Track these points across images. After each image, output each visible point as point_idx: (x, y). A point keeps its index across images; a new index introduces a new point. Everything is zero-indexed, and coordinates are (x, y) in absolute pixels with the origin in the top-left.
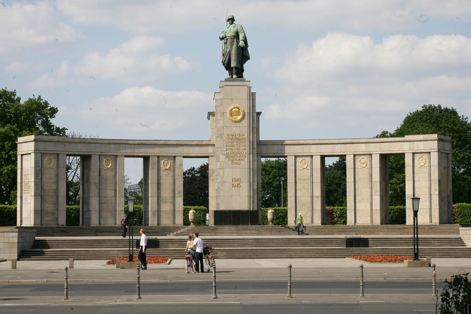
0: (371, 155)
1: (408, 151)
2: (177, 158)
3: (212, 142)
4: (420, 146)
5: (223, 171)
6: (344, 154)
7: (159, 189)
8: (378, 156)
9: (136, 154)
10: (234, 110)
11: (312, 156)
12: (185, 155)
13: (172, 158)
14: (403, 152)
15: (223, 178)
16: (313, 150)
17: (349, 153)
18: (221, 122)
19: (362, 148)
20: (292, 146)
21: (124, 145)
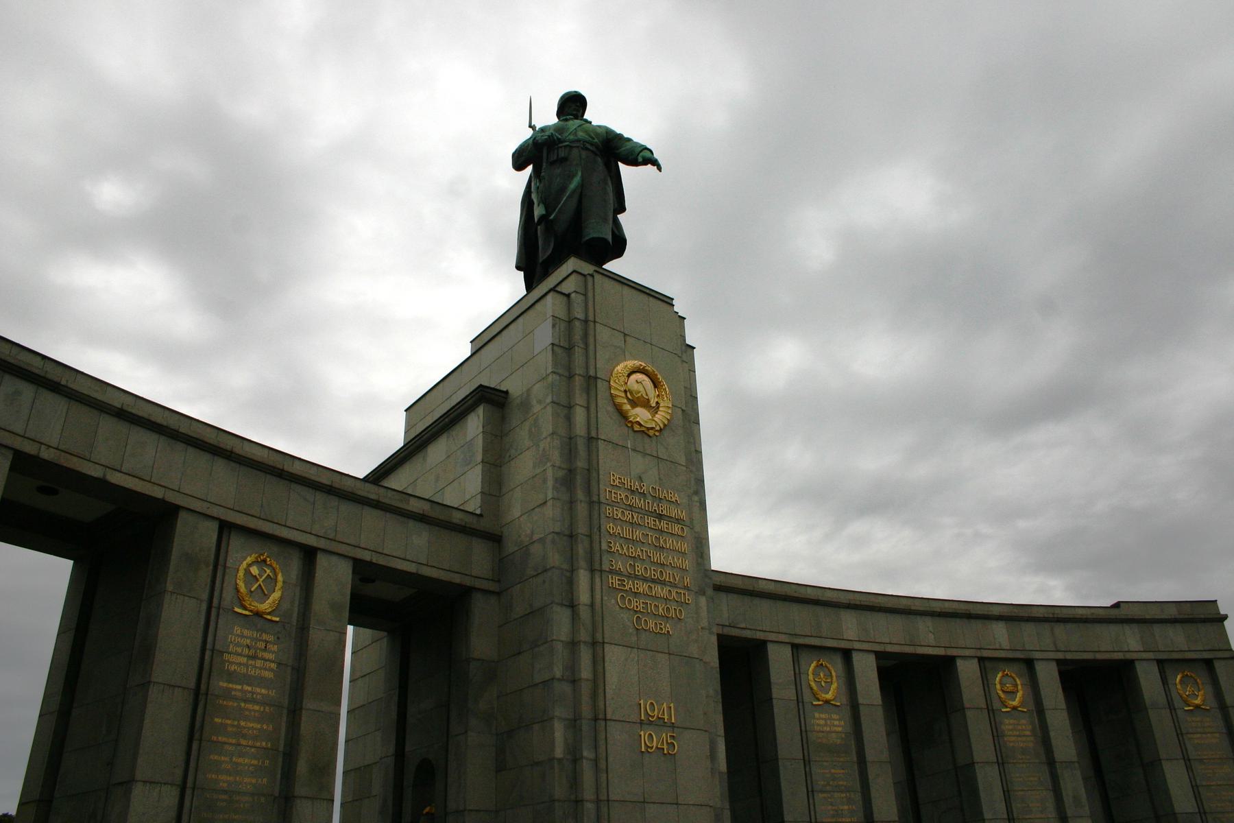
0: (1029, 663)
1: (1145, 656)
2: (322, 561)
3: (484, 525)
4: (1176, 640)
5: (598, 662)
6: (950, 652)
7: (194, 733)
8: (1053, 668)
9: (96, 472)
10: (634, 377)
11: (847, 654)
12: (366, 556)
13: (295, 565)
14: (1129, 656)
15: (594, 695)
16: (850, 628)
17: (967, 653)
18: (580, 415)
19: (1000, 635)
20: (780, 604)
21: (27, 390)
